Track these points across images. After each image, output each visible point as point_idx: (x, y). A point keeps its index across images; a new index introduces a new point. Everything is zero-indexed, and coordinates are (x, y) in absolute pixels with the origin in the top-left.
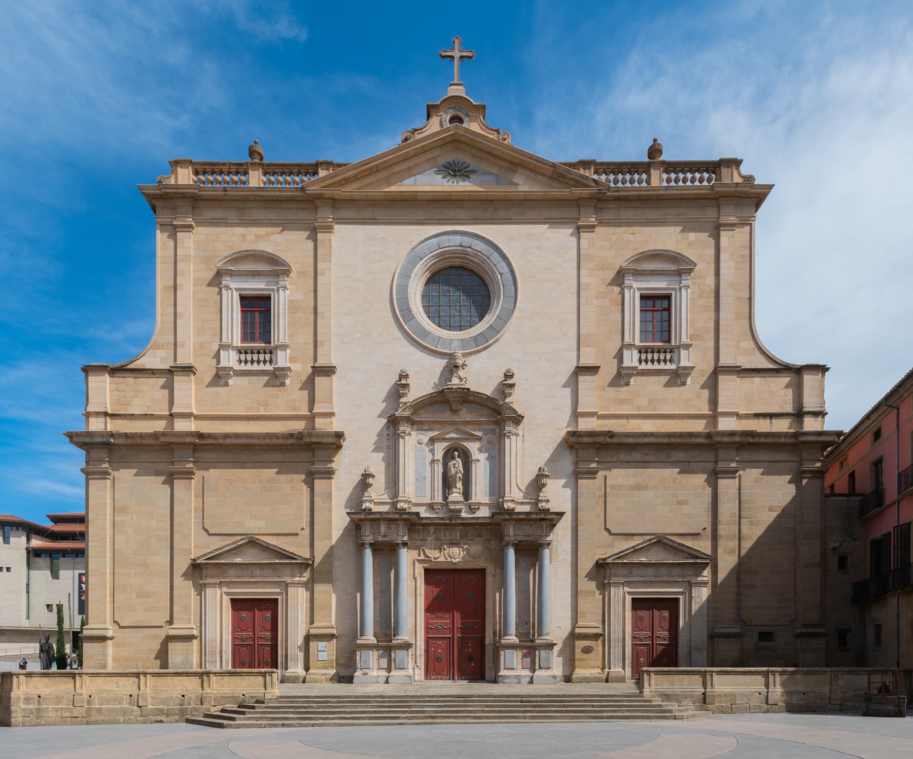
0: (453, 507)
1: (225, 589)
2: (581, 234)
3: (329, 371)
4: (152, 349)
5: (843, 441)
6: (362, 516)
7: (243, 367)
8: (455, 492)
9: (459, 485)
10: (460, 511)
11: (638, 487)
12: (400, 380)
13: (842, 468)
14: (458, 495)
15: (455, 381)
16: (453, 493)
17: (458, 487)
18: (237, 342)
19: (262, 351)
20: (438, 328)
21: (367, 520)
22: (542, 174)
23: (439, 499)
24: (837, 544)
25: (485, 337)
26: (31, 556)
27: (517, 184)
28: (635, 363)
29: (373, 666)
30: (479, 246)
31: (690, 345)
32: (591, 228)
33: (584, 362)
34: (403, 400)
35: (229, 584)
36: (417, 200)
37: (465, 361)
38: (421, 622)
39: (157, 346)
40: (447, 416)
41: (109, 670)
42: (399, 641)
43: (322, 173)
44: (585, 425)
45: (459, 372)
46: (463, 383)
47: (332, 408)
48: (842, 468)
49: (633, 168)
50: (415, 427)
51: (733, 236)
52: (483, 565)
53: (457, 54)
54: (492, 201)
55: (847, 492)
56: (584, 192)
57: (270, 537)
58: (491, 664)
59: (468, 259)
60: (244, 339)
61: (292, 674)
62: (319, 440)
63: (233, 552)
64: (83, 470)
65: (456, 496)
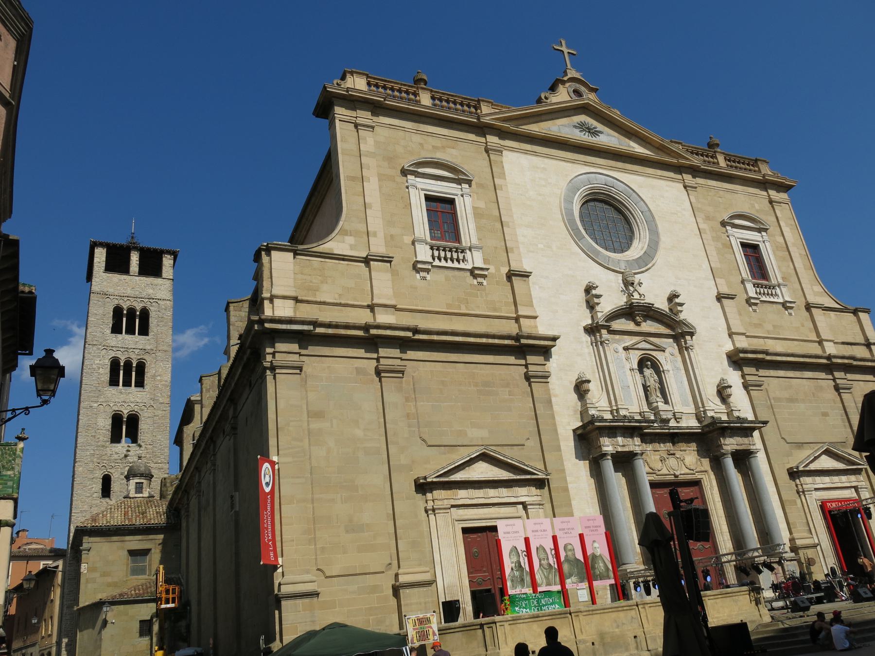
4: (340, 235)
39: (344, 232)
52: (699, 477)
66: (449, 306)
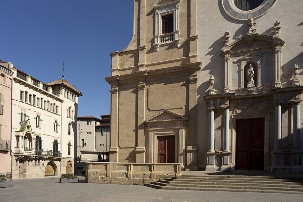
0: (249, 90)
7: (163, 43)
9: (252, 79)
10: (253, 91)
14: (252, 84)
15: (250, 32)
16: (249, 84)
17: (252, 81)
18: (160, 33)
20: (242, 11)
21: (212, 99)
23: (242, 87)
34: (226, 44)
37: (255, 22)
40: (246, 49)
46: (254, 32)
50: (232, 56)
57: (172, 110)
62: (191, 68)
63: (159, 117)
64: (110, 91)
65: (251, 84)
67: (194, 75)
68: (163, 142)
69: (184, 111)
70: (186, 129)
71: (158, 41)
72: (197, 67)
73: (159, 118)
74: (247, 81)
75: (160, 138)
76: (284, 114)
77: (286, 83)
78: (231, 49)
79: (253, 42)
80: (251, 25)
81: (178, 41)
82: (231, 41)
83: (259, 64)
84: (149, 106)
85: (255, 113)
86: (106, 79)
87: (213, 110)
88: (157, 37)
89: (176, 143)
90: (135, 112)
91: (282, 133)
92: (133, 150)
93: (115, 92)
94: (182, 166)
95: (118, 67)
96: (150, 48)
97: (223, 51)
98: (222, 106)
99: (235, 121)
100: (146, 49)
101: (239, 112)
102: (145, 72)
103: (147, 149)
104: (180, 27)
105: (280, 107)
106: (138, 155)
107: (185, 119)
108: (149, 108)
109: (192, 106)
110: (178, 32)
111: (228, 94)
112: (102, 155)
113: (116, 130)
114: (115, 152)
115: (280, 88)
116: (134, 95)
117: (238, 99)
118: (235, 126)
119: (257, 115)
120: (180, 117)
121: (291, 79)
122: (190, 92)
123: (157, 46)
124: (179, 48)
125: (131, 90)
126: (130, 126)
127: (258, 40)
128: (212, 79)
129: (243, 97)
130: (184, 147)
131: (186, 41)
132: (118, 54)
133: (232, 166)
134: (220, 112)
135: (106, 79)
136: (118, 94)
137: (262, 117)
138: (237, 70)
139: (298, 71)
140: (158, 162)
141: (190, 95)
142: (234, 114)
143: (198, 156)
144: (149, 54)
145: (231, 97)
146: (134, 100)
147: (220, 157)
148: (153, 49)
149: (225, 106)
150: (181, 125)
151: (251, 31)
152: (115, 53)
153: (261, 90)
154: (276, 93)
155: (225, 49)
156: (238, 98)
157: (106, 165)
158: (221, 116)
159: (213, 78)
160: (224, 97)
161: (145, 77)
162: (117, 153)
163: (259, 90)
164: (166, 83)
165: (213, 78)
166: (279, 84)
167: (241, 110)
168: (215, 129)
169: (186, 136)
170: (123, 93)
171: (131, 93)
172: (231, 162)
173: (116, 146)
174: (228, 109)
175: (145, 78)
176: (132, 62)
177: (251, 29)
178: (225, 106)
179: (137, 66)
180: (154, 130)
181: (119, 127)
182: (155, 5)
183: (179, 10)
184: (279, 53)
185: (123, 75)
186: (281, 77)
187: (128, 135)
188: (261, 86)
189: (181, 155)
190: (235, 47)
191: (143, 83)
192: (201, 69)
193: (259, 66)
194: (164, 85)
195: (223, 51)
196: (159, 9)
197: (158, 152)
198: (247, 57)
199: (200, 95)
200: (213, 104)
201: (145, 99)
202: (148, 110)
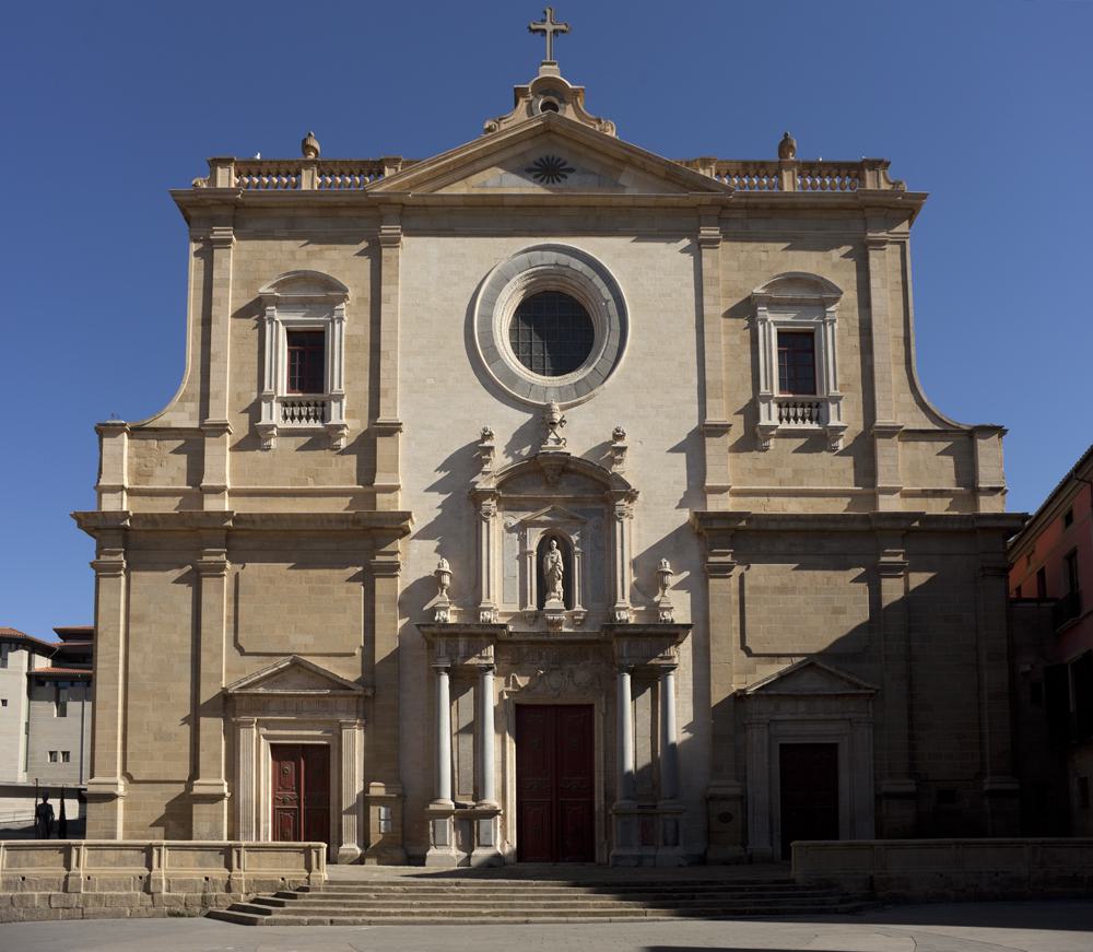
0: (551, 618)
1: (264, 731)
2: (703, 250)
3: (392, 430)
5: (1030, 525)
6: (435, 630)
7: (289, 424)
8: (554, 597)
9: (559, 586)
10: (559, 623)
11: (783, 590)
12: (482, 441)
13: (1029, 563)
14: (556, 600)
15: (551, 444)
18: (283, 389)
19: (312, 404)
20: (530, 372)
21: (442, 635)
22: (651, 173)
23: (532, 607)
24: (1028, 668)
25: (588, 384)
26: (34, 683)
27: (624, 187)
28: (775, 421)
29: (451, 842)
30: (579, 265)
31: (840, 398)
32: (713, 243)
33: (711, 419)
34: (486, 468)
35: (266, 725)
36: (503, 206)
38: (512, 780)
40: (540, 492)
41: (120, 840)
42: (484, 807)
43: (388, 172)
44: (716, 504)
45: (556, 431)
46: (561, 445)
47: (397, 480)
48: (1029, 563)
49: (761, 168)
50: (502, 506)
51: (884, 257)
53: (549, 27)
54: (594, 207)
55: (1035, 596)
56: (704, 198)
57: (319, 658)
58: (603, 839)
59: (565, 282)
60: (292, 388)
61: (349, 852)
62: (379, 525)
63: (275, 678)
64: (92, 565)
65: (555, 602)
66: (296, 481)
67: (388, 548)
68: (289, 767)
69: (360, 665)
70: (365, 727)
71: (273, 415)
72: (397, 525)
73: (276, 681)
74: (544, 591)
75: (277, 751)
76: (640, 699)
77: (643, 608)
78: (499, 486)
79: (559, 475)
80: (555, 424)
81: (340, 427)
82: (499, 462)
83: (577, 545)
84: (240, 635)
85: (567, 688)
86: (75, 516)
87: (447, 670)
88: (269, 399)
89: (333, 772)
90: (188, 651)
91: (634, 753)
92: (181, 789)
93: (113, 570)
94: (351, 847)
95: (126, 478)
96: (247, 432)
97: (477, 486)
98: (473, 661)
99: (512, 707)
100: (230, 433)
101: (522, 681)
102: (226, 515)
103: (234, 788)
104: (347, 383)
105: (628, 678)
106: (199, 810)
107: (361, 693)
108: (240, 642)
109: (383, 649)
110: (339, 398)
111: (489, 624)
112: (55, 803)
113: (117, 714)
114: (112, 797)
115: (625, 624)
116: (186, 592)
117: (520, 642)
118: (513, 729)
119: (572, 697)
120: (345, 683)
121: (656, 599)
122: (377, 605)
123: (269, 430)
124: (343, 452)
125: (176, 573)
126: (172, 701)
127: (572, 472)
128: (444, 572)
129: (532, 638)
130: (359, 787)
131: (366, 433)
132: (126, 430)
133: (507, 849)
134: (467, 680)
135: (75, 516)
136: (123, 579)
137: (585, 702)
138: (518, 553)
139: (672, 580)
140: (274, 839)
141: (377, 614)
142: (510, 689)
143: (403, 819)
144: (241, 453)
145: (494, 634)
146: (188, 609)
147: (470, 822)
148: (255, 438)
149: (480, 661)
150: (348, 712)
151: (555, 440)
152: (114, 425)
153: (583, 621)
154: (618, 635)
155: (484, 483)
156: (518, 638)
157: (67, 850)
158: (472, 689)
159: (446, 567)
160: (479, 633)
161: (224, 532)
162: (120, 802)
163: (578, 620)
164: (301, 565)
165: (446, 567)
166: (628, 613)
167: (528, 678)
168: (455, 730)
169: (367, 749)
170: (142, 578)
171: (178, 581)
172: (502, 839)
173: (115, 775)
174: (491, 672)
175: (228, 538)
176: (179, 468)
177: (552, 436)
178: (480, 661)
179: (197, 490)
180: (260, 724)
181: (129, 703)
182: (264, 289)
183: (344, 324)
184: (626, 520)
185: (146, 515)
186: (631, 589)
187: (161, 736)
188: (582, 609)
189: (350, 811)
190: (510, 480)
191: (219, 554)
192: (413, 534)
193: (577, 549)
194: (293, 571)
195: (477, 486)
196: (277, 305)
197: (274, 800)
198: (544, 518)
199: (408, 619)
200: (446, 651)
201: (226, 611)
202: (237, 651)
